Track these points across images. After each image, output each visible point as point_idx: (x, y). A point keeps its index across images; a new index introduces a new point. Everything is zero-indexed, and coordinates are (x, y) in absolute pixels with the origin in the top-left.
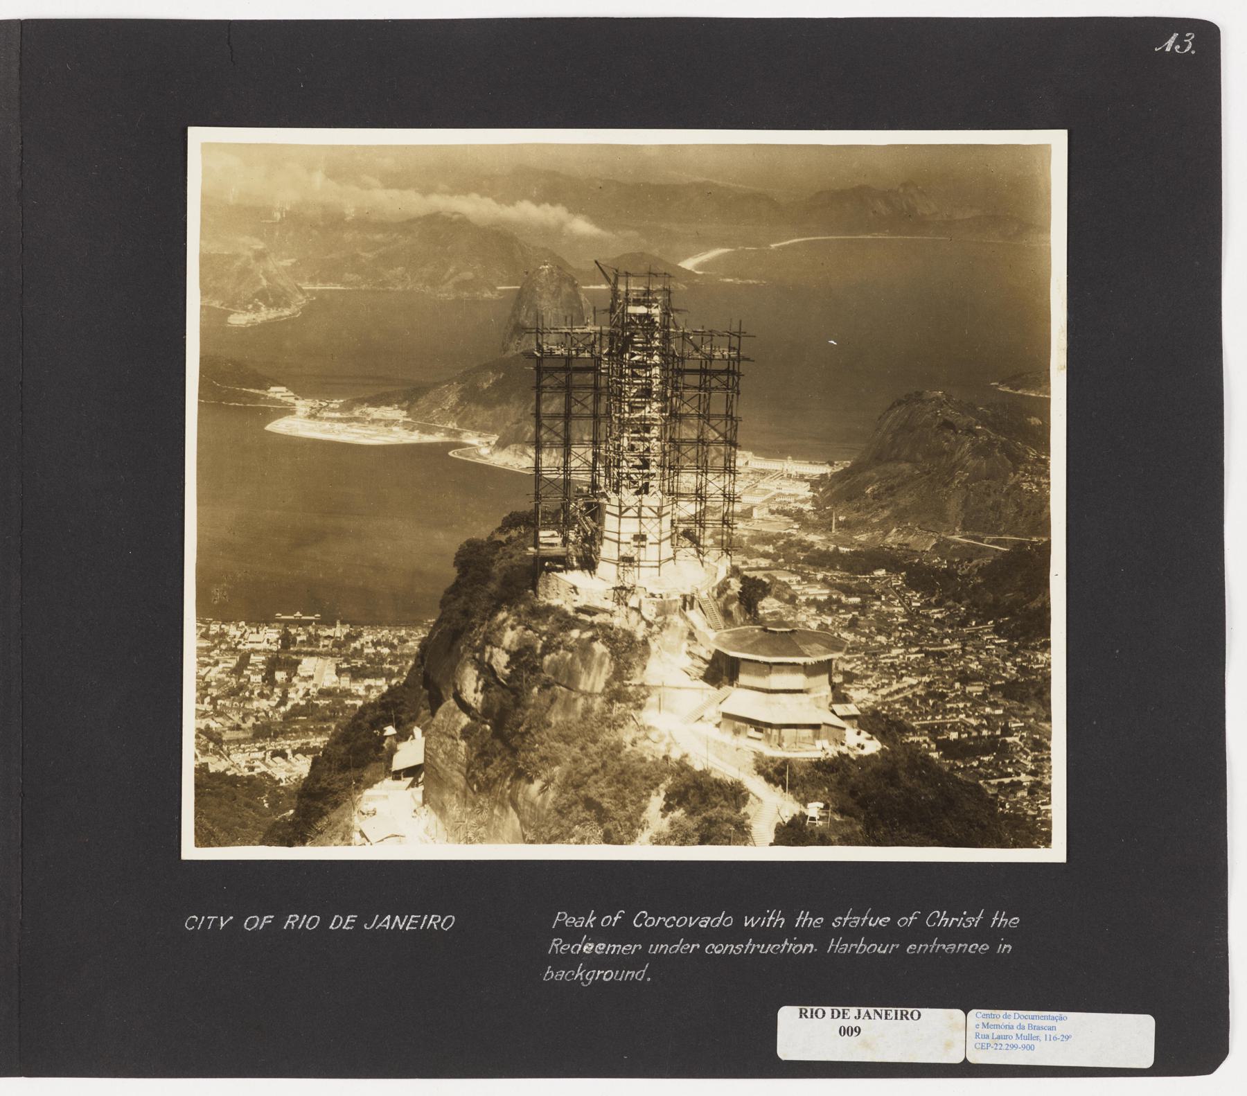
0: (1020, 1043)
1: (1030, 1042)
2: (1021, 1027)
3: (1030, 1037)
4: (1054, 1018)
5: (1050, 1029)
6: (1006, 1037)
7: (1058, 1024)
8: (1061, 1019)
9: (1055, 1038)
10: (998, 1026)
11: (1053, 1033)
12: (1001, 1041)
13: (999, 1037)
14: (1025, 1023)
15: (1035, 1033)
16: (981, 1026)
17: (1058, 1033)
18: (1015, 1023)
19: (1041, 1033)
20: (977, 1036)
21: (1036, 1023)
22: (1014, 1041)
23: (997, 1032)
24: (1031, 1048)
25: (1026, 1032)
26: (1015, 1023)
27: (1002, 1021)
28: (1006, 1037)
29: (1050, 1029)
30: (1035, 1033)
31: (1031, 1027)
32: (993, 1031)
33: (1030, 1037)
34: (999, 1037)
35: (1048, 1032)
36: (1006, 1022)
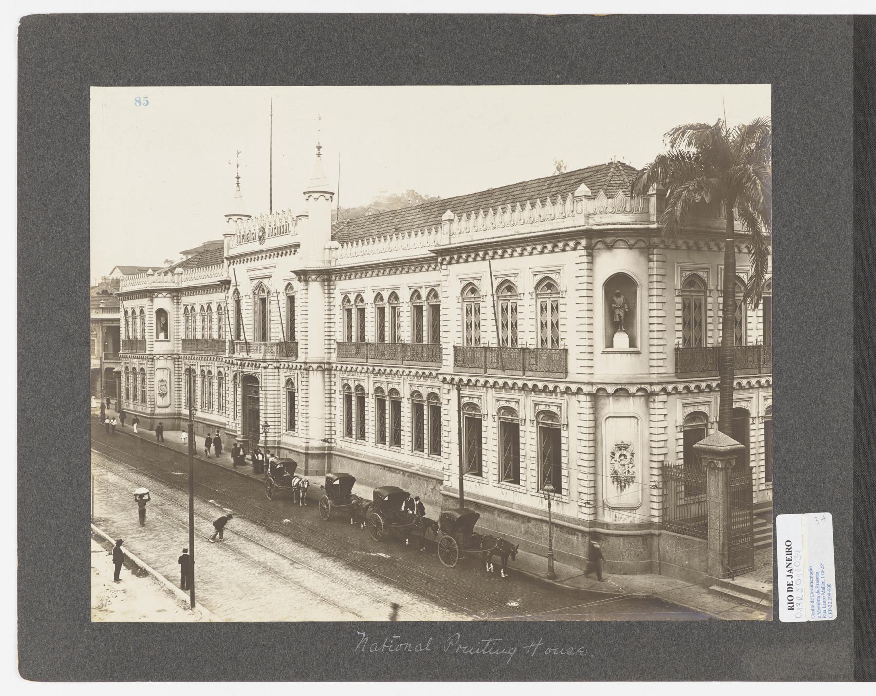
0: (827, 592)
1: (826, 586)
2: (818, 592)
3: (823, 587)
4: (811, 574)
5: (817, 575)
6: (824, 601)
7: (815, 571)
8: (811, 569)
9: (823, 572)
10: (819, 605)
11: (820, 574)
12: (827, 601)
13: (825, 604)
14: (815, 590)
15: (820, 584)
16: (819, 615)
17: (820, 570)
18: (816, 595)
19: (821, 580)
20: (825, 617)
21: (815, 584)
22: (826, 596)
23: (822, 605)
24: (829, 585)
25: (821, 589)
26: (816, 595)
27: (815, 604)
28: (824, 601)
29: (817, 575)
30: (820, 584)
31: (817, 587)
32: (821, 608)
33: (823, 587)
34: (825, 604)
35: (820, 576)
36: (815, 601)
